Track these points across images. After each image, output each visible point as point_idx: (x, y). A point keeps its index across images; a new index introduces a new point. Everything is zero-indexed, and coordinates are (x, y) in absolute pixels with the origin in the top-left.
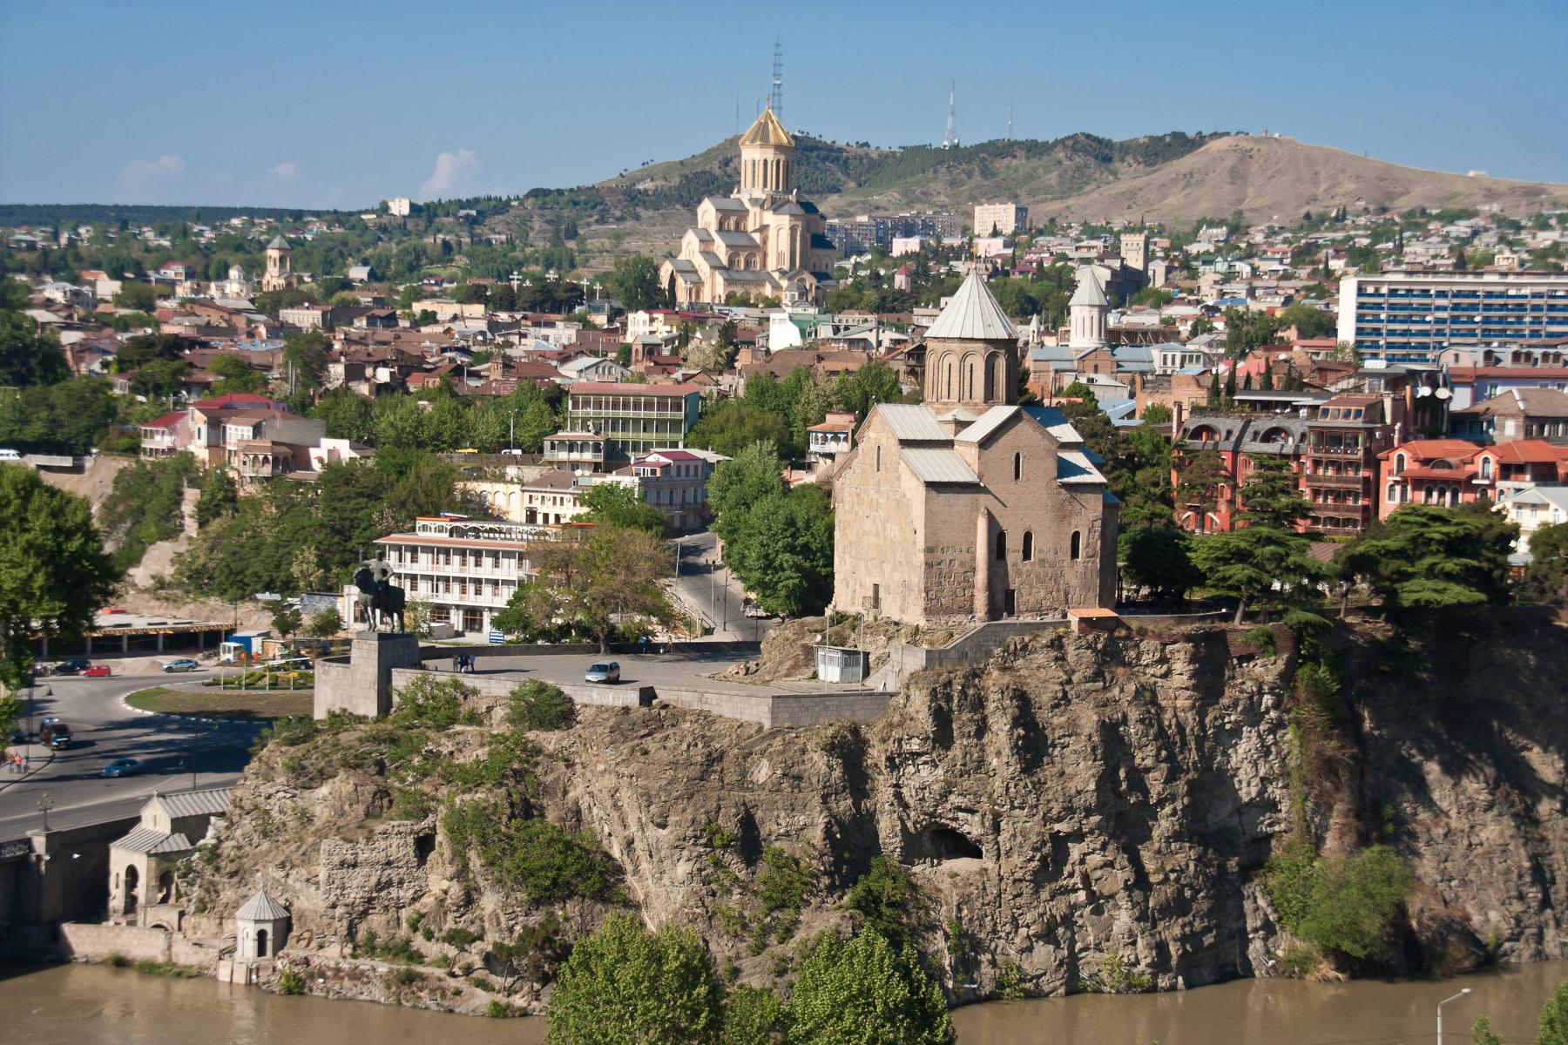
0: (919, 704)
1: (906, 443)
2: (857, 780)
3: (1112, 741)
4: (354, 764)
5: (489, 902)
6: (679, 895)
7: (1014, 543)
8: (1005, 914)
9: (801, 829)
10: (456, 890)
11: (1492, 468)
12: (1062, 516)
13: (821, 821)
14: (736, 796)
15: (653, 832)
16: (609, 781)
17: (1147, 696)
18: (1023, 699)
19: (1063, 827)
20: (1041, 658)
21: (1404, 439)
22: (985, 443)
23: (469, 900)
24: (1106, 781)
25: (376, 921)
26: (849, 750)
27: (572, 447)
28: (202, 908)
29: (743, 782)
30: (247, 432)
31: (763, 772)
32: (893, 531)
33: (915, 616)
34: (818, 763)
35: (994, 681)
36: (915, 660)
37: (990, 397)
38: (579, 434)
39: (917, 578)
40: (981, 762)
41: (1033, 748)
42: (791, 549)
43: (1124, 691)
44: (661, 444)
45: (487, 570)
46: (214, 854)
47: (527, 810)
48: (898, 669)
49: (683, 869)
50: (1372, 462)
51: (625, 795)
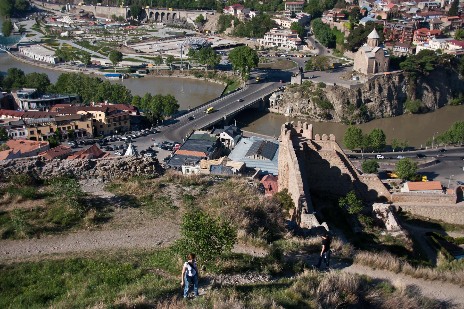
0: (367, 86)
1: (366, 52)
2: (360, 94)
3: (389, 88)
4: (299, 91)
5: (318, 109)
6: (340, 109)
7: (378, 64)
8: (375, 110)
9: (354, 101)
10: (313, 108)
11: (429, 34)
12: (384, 60)
13: (356, 100)
14: (347, 97)
15: (337, 102)
16: (331, 95)
17: (393, 83)
18: (380, 85)
19: (383, 99)
20: (381, 79)
21: (418, 29)
22: (376, 52)
23: (315, 109)
24: (388, 94)
25: (303, 110)
26: (359, 91)
27: (287, 13)
28: (281, 106)
29: (347, 95)
30: (240, 11)
31: (349, 94)
32: (363, 62)
33: (366, 73)
34: (356, 93)
35: (376, 83)
36: (367, 80)
37: (376, 45)
38: (287, 11)
39: (366, 69)
40: (374, 92)
41: (381, 90)
42: (327, 38)
43: (390, 82)
44: (299, 12)
45: (282, 38)
46: (282, 100)
47: (322, 99)
48: (364, 81)
49: (341, 106)
50: (413, 32)
51: (333, 97)
